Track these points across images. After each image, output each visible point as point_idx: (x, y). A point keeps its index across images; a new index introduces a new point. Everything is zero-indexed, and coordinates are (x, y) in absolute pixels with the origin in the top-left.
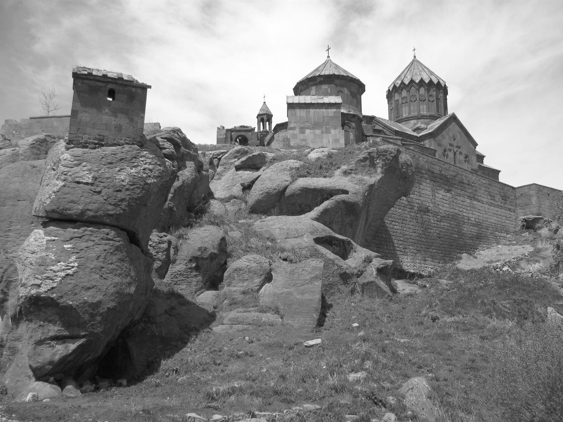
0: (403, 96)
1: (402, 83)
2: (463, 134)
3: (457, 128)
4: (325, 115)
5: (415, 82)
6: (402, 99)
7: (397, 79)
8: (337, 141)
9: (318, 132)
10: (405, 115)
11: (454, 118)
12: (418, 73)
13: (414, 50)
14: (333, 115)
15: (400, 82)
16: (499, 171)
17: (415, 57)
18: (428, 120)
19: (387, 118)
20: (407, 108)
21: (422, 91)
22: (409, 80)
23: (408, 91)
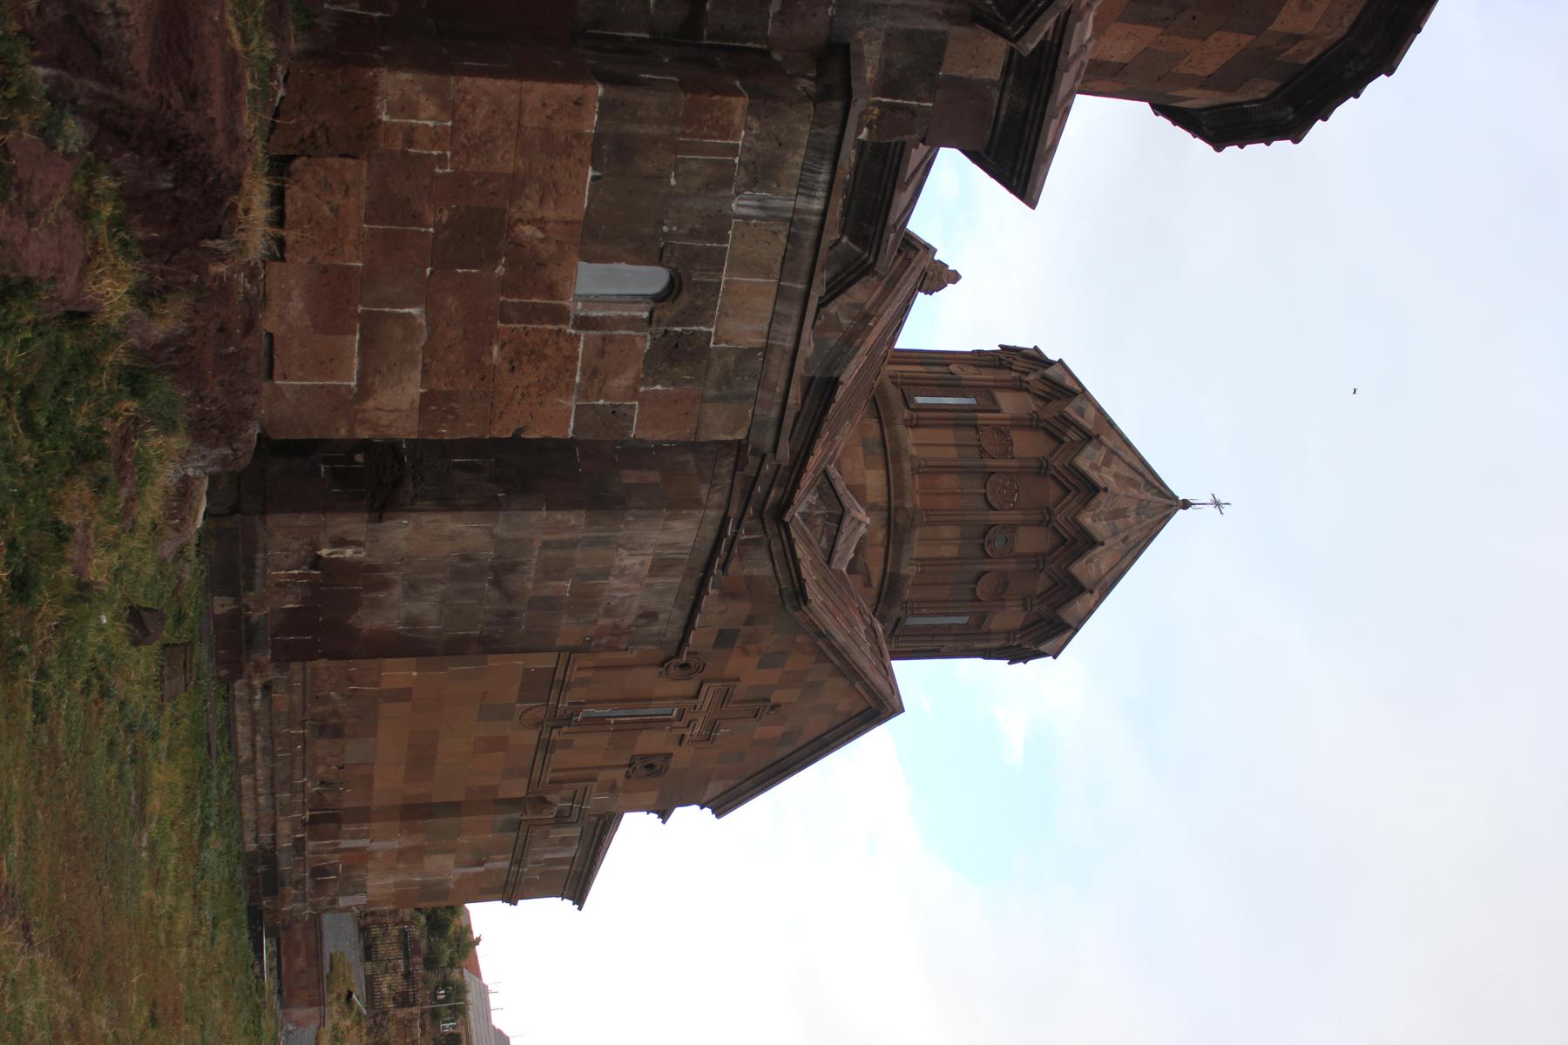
0: (1015, 435)
1: (1088, 437)
3: (816, 725)
5: (1085, 505)
6: (1002, 431)
10: (910, 437)
11: (879, 706)
13: (1217, 504)
15: (1088, 422)
16: (579, 899)
17: (1186, 505)
18: (876, 573)
19: (902, 343)
20: (952, 453)
21: (1031, 541)
22: (1094, 475)
23: (1042, 469)
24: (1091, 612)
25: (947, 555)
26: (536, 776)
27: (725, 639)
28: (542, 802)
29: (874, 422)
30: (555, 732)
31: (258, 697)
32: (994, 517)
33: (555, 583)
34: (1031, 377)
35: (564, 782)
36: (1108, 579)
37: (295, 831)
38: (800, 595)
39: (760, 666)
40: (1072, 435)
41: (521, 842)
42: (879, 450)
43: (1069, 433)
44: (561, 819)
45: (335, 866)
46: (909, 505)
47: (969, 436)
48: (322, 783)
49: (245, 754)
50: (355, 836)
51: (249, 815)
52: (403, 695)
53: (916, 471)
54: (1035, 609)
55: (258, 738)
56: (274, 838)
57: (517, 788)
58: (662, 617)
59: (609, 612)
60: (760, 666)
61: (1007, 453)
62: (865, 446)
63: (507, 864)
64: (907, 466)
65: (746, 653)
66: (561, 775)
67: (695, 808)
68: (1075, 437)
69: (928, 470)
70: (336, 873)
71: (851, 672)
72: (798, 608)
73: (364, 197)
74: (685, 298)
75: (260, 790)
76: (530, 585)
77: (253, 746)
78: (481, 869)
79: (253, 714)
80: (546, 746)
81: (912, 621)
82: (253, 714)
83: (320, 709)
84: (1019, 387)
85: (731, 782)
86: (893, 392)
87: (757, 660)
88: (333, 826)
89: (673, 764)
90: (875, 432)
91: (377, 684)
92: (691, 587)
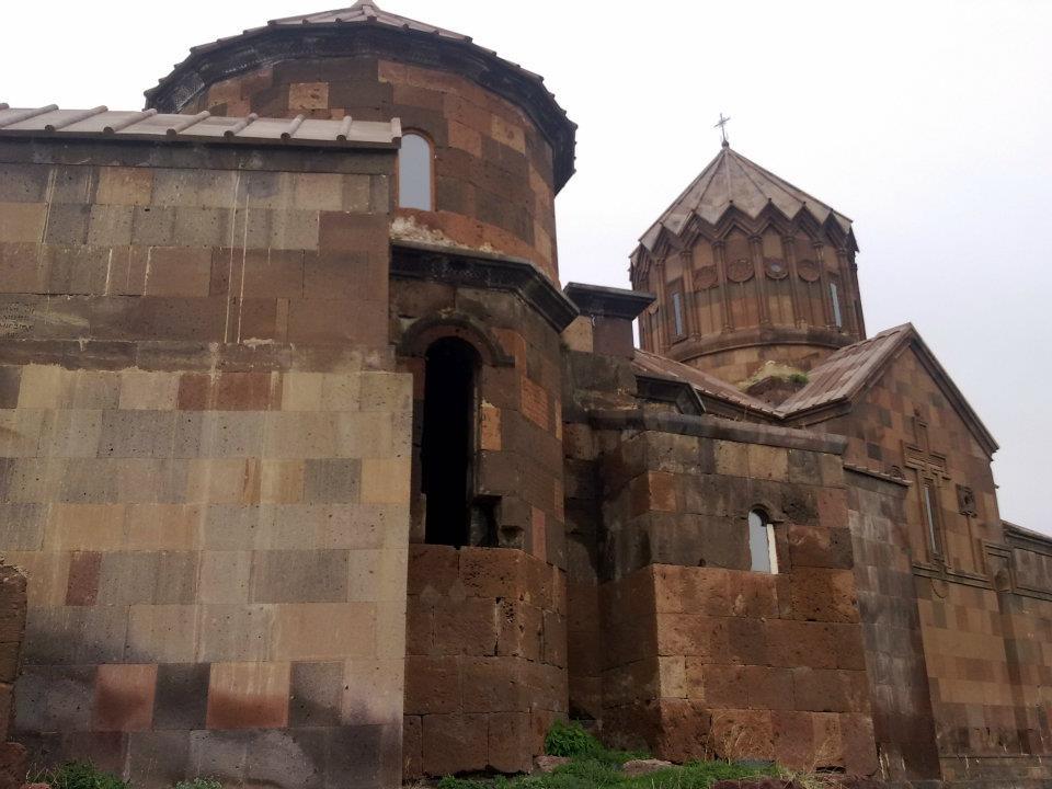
1: (695, 217)
2: (947, 405)
3: (927, 383)
4: (243, 236)
5: (743, 214)
6: (697, 275)
7: (672, 209)
8: (332, 479)
9: (147, 388)
10: (709, 335)
12: (751, 188)
14: (309, 240)
15: (683, 218)
18: (806, 351)
20: (716, 307)
21: (772, 246)
23: (720, 246)
24: (817, 201)
25: (790, 303)
27: (875, 452)
28: (999, 579)
29: (700, 361)
30: (950, 572)
32: (760, 275)
33: (870, 577)
34: (655, 259)
35: (983, 563)
36: (792, 192)
38: (840, 404)
39: (890, 425)
40: (694, 228)
41: (1028, 593)
42: (720, 357)
43: (693, 229)
44: (1010, 563)
46: (758, 333)
47: (701, 296)
48: (1000, 744)
53: (732, 330)
54: (821, 239)
57: (990, 598)
58: (884, 499)
59: (885, 538)
60: (890, 425)
61: (711, 270)
62: (718, 366)
64: (730, 336)
65: (883, 437)
66: (979, 566)
67: (992, 465)
68: (695, 226)
69: (729, 322)
71: (887, 362)
72: (849, 403)
73: (733, 710)
74: (765, 502)
76: (873, 594)
80: (960, 578)
81: (839, 323)
84: (662, 267)
85: (972, 440)
86: (676, 349)
87: (886, 428)
89: (964, 484)
90: (708, 360)
92: (863, 481)
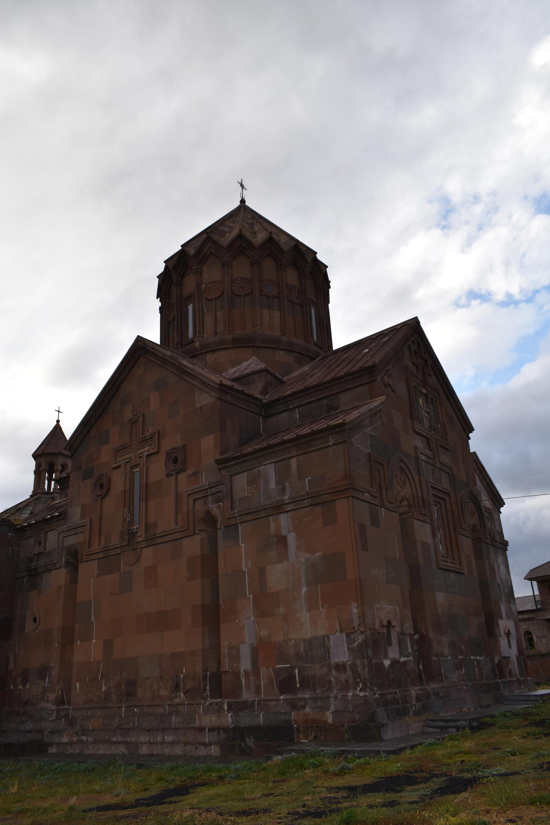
26: (179, 535)
31: (84, 738)
37: (220, 710)
41: (250, 517)
45: (278, 672)
49: (122, 749)
50: (237, 658)
51: (179, 750)
52: (108, 645)
55: (114, 739)
56: (211, 730)
63: (283, 517)
70: (292, 668)
75: (159, 739)
77: (115, 743)
78: (291, 539)
79: (96, 742)
82: (96, 742)
83: (114, 697)
88: (225, 678)
91: (99, 663)
